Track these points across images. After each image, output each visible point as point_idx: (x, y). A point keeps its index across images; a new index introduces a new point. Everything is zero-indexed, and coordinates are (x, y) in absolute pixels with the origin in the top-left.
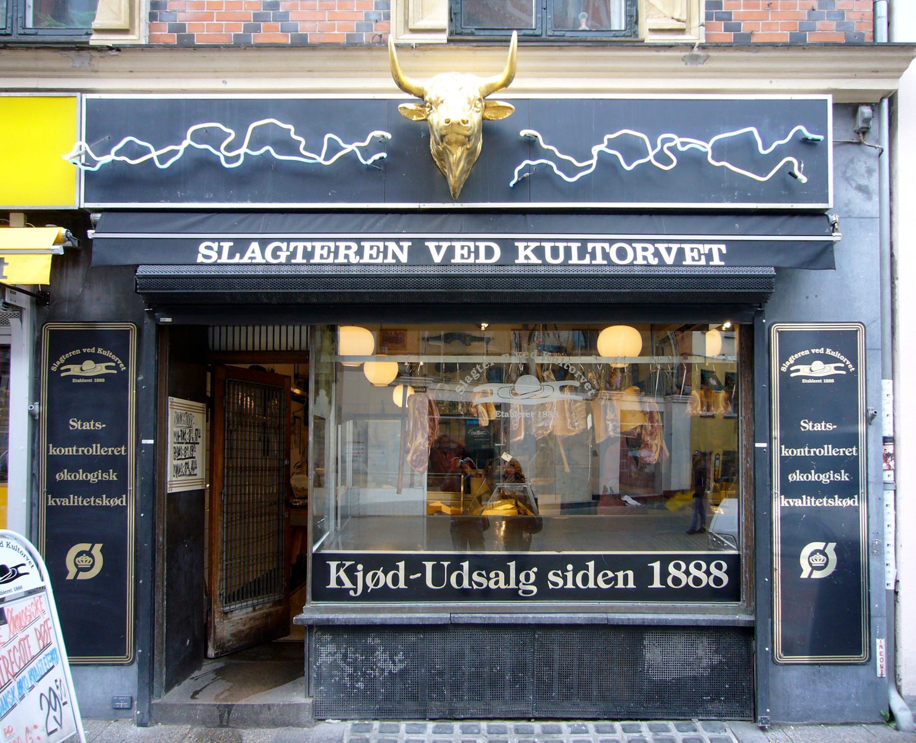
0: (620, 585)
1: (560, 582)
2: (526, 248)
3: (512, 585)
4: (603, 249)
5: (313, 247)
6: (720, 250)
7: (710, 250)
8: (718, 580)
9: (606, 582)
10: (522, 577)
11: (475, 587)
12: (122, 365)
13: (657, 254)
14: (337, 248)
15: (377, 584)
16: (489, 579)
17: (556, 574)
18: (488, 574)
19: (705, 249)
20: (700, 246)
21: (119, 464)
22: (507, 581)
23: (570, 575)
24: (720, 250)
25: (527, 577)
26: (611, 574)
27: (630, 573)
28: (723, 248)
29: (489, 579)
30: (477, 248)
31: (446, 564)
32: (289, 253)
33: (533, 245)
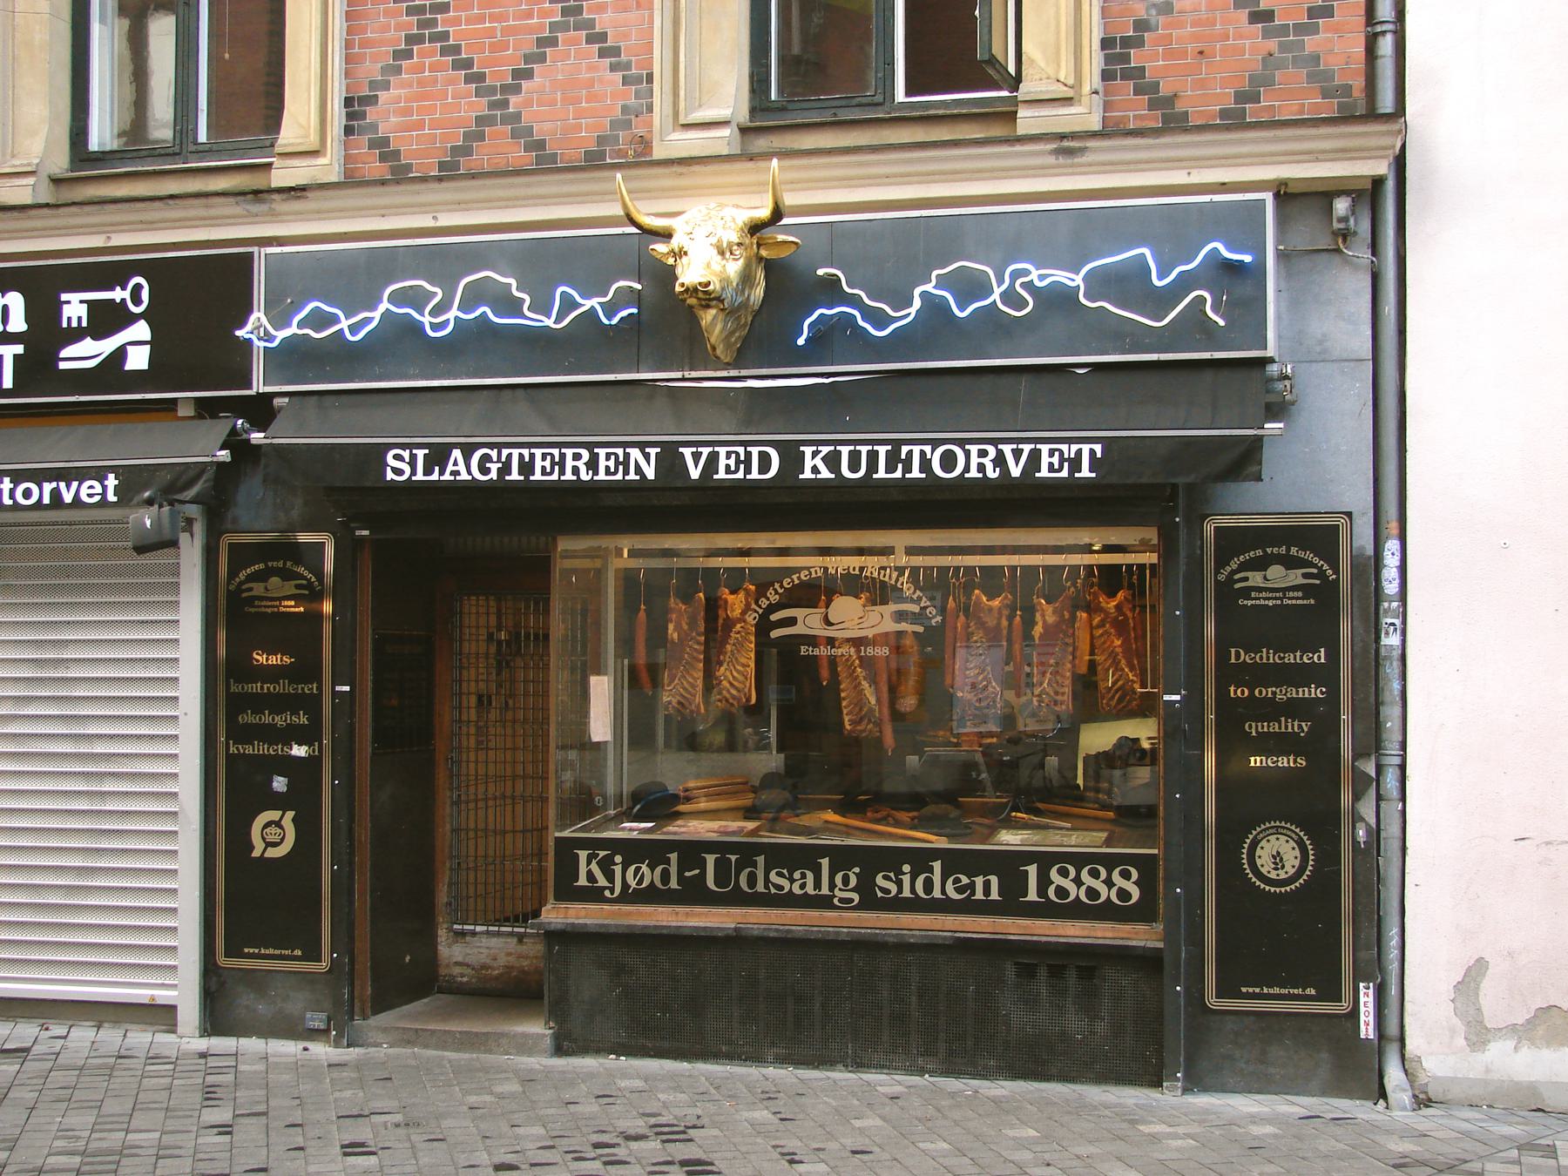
1: (893, 888)
3: (825, 890)
4: (923, 453)
23: (906, 879)
30: (748, 455)
33: (825, 450)
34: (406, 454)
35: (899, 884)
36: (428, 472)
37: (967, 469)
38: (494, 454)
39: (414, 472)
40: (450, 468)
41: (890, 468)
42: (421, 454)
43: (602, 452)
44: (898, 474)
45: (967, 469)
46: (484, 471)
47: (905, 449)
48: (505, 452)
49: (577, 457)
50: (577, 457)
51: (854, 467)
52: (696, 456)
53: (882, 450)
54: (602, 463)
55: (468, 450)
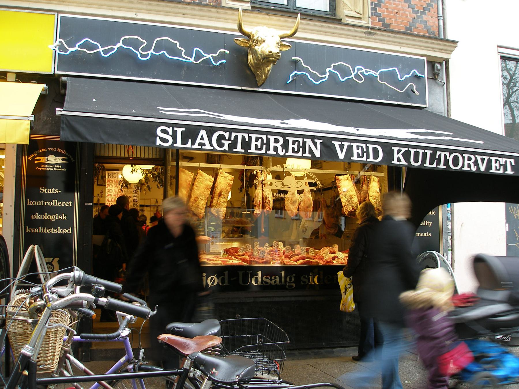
1: (307, 281)
2: (399, 151)
4: (445, 156)
5: (250, 138)
6: (511, 162)
7: (506, 162)
10: (288, 279)
11: (264, 284)
12: (72, 159)
13: (476, 163)
14: (268, 140)
15: (213, 283)
18: (271, 277)
19: (502, 161)
20: (500, 159)
21: (69, 211)
24: (511, 162)
25: (290, 279)
29: (271, 280)
30: (368, 148)
32: (230, 142)
33: (404, 150)
34: (170, 130)
36: (184, 142)
37: (463, 166)
38: (227, 135)
39: (175, 141)
40: (198, 141)
41: (431, 163)
42: (179, 131)
43: (291, 140)
44: (434, 165)
45: (463, 166)
46: (221, 145)
47: (438, 153)
48: (233, 135)
50: (276, 141)
51: (416, 161)
52: (342, 147)
53: (429, 152)
54: (291, 146)
55: (210, 131)
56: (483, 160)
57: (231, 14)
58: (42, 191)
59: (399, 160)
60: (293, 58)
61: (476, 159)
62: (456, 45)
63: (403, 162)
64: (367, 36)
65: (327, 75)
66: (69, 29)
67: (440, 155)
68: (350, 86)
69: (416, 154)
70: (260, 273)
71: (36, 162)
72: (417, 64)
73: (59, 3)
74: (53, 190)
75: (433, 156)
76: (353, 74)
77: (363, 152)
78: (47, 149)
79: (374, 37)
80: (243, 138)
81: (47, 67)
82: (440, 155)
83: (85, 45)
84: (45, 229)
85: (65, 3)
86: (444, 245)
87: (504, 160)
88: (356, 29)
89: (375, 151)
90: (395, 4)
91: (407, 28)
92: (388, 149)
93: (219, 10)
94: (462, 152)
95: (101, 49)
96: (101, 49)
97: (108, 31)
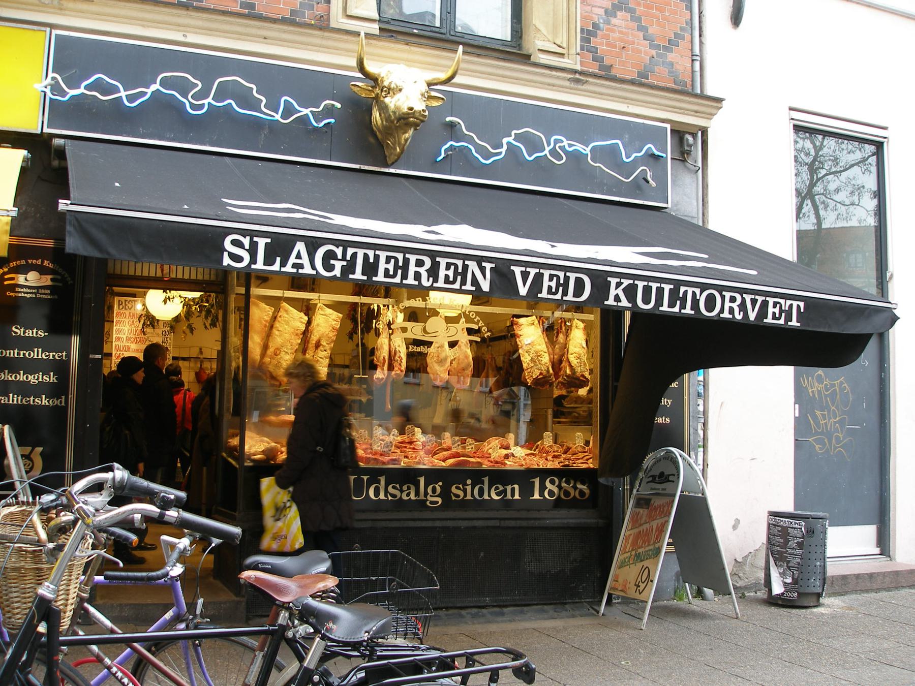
0: (509, 497)
1: (461, 494)
2: (618, 285)
3: (422, 497)
4: (694, 293)
5: (377, 257)
6: (798, 306)
7: (791, 305)
8: (582, 493)
9: (498, 494)
12: (69, 279)
13: (743, 306)
14: (406, 261)
16: (402, 491)
17: (457, 488)
18: (401, 487)
20: (782, 301)
22: (417, 493)
23: (469, 488)
24: (798, 306)
26: (501, 488)
27: (516, 487)
28: (802, 304)
29: (402, 491)
30: (567, 279)
31: (365, 478)
32: (345, 263)
33: (626, 282)
34: (246, 241)
35: (465, 491)
36: (269, 261)
37: (722, 311)
38: (339, 252)
39: (253, 260)
40: (292, 260)
41: (672, 305)
42: (262, 242)
44: (676, 309)
45: (722, 311)
46: (329, 267)
47: (683, 289)
49: (420, 263)
50: (420, 263)
51: (646, 301)
52: (525, 275)
53: (667, 288)
54: (442, 272)
55: (313, 245)
56: (754, 302)
57: (347, 42)
58: (16, 333)
59: (617, 298)
60: (448, 119)
61: (743, 300)
62: (719, 105)
63: (625, 303)
64: (572, 85)
65: (504, 150)
66: (70, 57)
67: (686, 292)
68: (542, 169)
69: (647, 290)
70: (422, 480)
71: (6, 283)
72: (654, 135)
73: (52, 10)
74: (35, 331)
75: (674, 294)
76: (547, 149)
77: (558, 285)
78: (27, 262)
79: (584, 87)
80: (366, 257)
81: (31, 121)
82: (686, 292)
83: (97, 86)
84: (20, 398)
85: (63, 12)
86: (692, 438)
87: (789, 302)
88: (554, 73)
89: (579, 284)
90: (620, 32)
91: (640, 75)
92: (600, 281)
93: (326, 34)
94: (721, 289)
95: (123, 94)
96: (123, 94)
97: (136, 62)
